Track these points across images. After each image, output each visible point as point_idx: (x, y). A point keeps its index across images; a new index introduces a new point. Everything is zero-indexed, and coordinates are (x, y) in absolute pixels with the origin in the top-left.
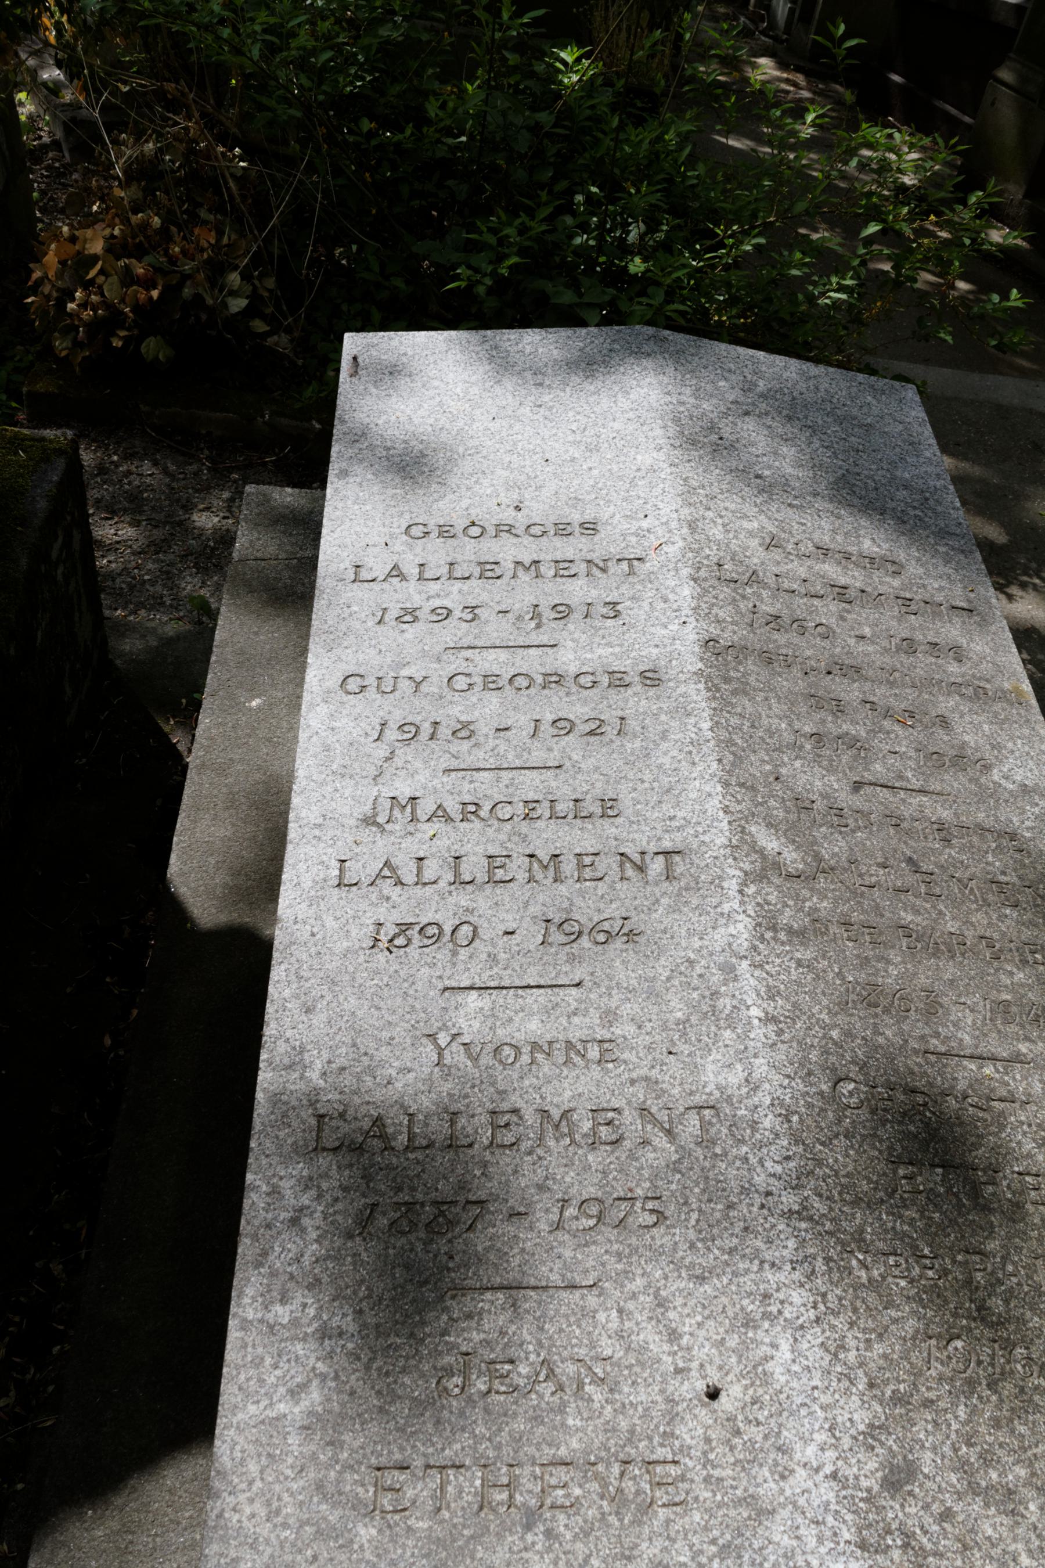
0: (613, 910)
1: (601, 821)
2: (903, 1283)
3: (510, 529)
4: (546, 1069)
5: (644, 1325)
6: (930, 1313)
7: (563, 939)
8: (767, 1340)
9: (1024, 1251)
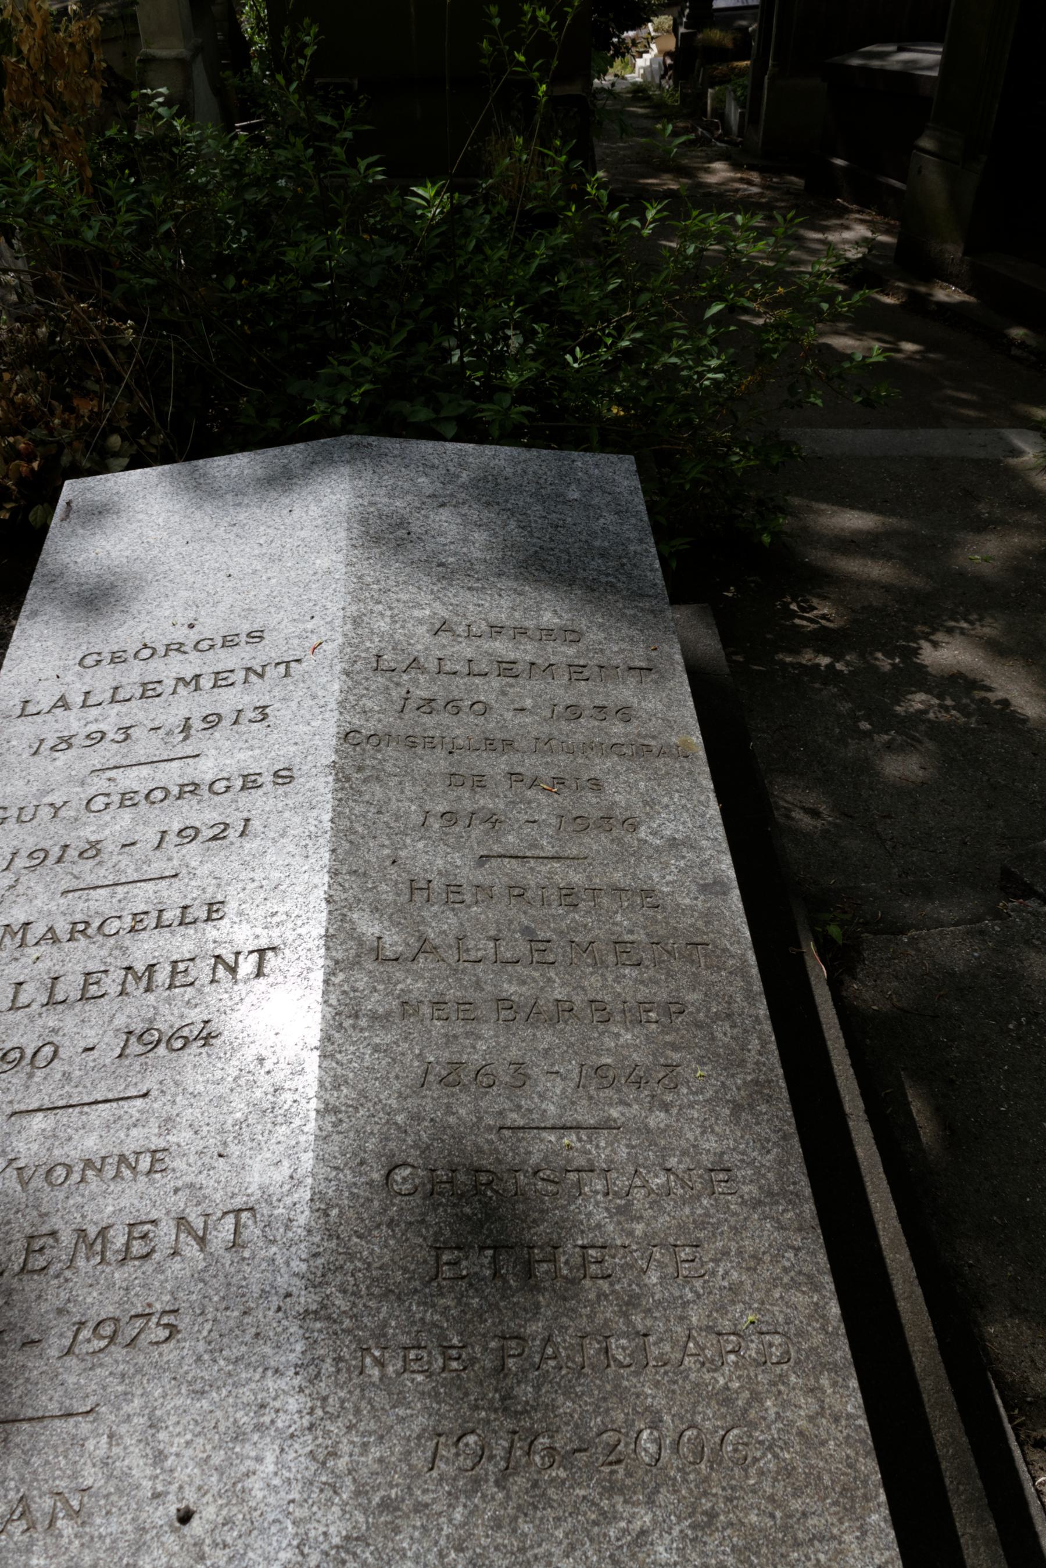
0: (195, 1015)
1: (203, 925)
2: (420, 1378)
3: (180, 648)
4: (93, 1186)
5: (131, 1449)
6: (445, 1408)
8: (253, 1454)
9: (570, 1331)
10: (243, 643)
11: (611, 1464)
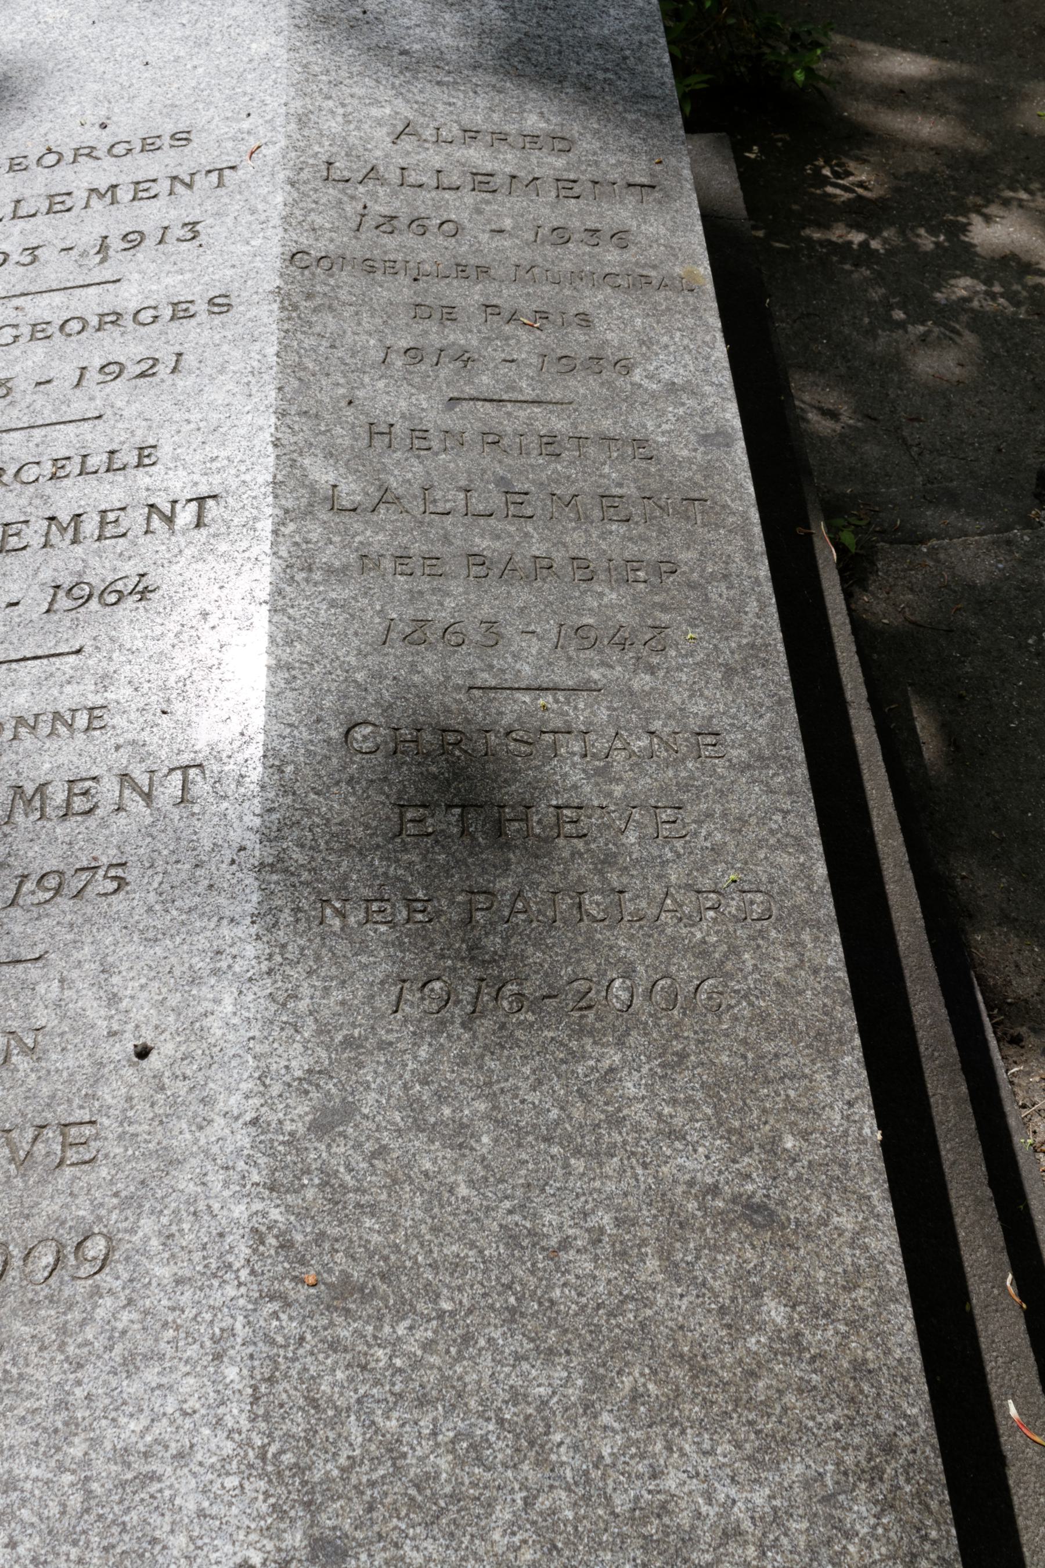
0: (130, 568)
1: (134, 471)
2: (383, 928)
3: (91, 153)
4: (27, 744)
5: (84, 992)
6: (408, 956)
7: (69, 604)
8: (211, 996)
10: (166, 147)
11: (581, 1009)
